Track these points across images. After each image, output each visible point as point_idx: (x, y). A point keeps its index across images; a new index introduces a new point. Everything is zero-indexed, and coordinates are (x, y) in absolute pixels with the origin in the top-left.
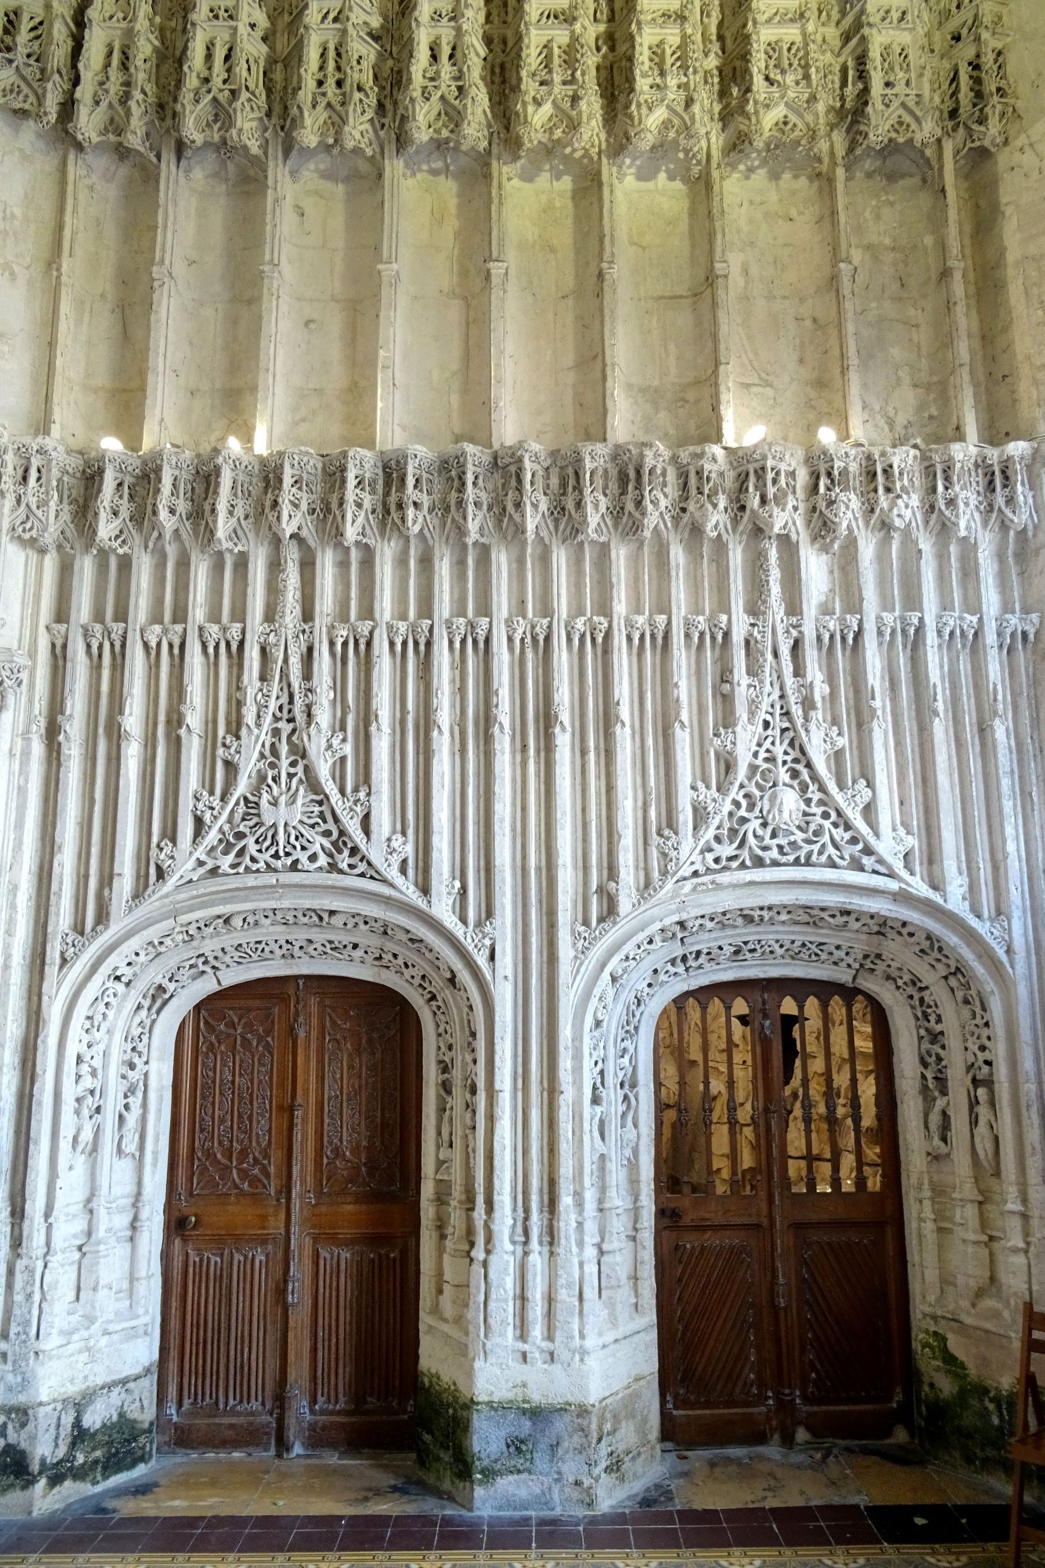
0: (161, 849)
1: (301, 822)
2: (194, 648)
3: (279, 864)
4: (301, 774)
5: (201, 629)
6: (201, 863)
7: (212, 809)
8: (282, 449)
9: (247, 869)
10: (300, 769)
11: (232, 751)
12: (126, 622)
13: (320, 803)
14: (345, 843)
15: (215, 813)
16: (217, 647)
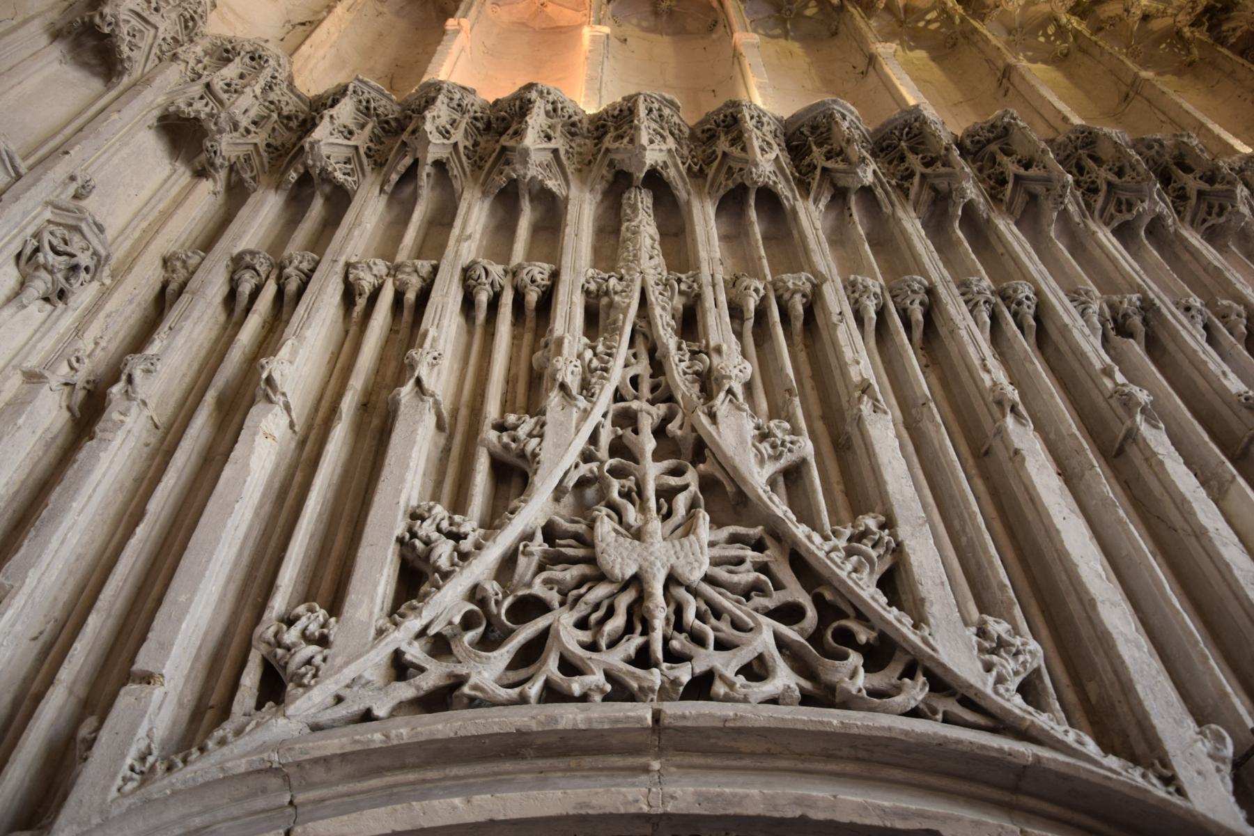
0: (290, 621)
1: (708, 579)
2: (448, 297)
3: (655, 677)
4: (694, 488)
5: (466, 271)
6: (400, 668)
7: (457, 537)
8: (633, 92)
9: (552, 694)
10: (691, 477)
11: (522, 432)
12: (321, 255)
13: (759, 546)
14: (846, 637)
15: (466, 545)
16: (494, 305)
